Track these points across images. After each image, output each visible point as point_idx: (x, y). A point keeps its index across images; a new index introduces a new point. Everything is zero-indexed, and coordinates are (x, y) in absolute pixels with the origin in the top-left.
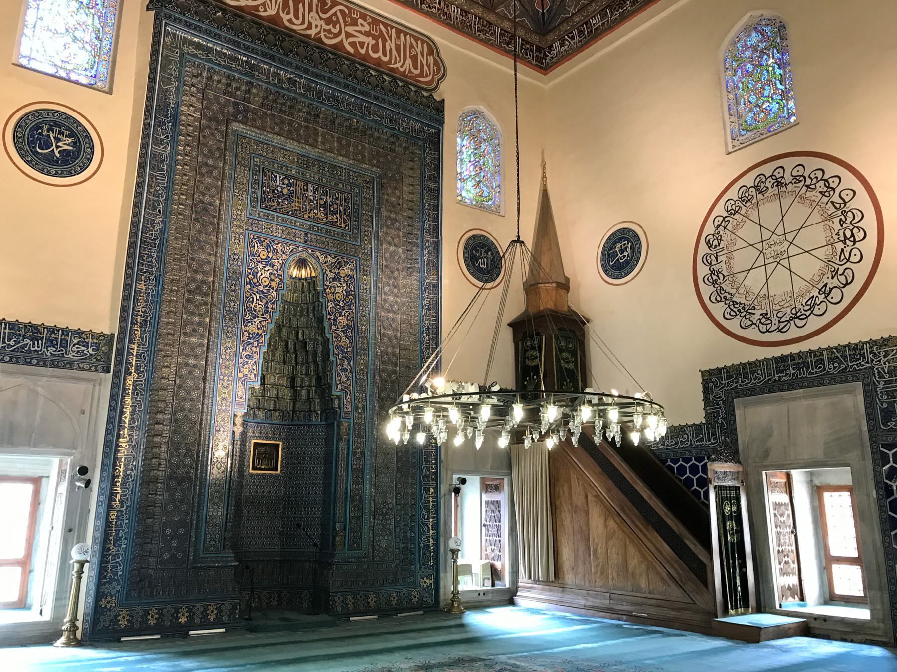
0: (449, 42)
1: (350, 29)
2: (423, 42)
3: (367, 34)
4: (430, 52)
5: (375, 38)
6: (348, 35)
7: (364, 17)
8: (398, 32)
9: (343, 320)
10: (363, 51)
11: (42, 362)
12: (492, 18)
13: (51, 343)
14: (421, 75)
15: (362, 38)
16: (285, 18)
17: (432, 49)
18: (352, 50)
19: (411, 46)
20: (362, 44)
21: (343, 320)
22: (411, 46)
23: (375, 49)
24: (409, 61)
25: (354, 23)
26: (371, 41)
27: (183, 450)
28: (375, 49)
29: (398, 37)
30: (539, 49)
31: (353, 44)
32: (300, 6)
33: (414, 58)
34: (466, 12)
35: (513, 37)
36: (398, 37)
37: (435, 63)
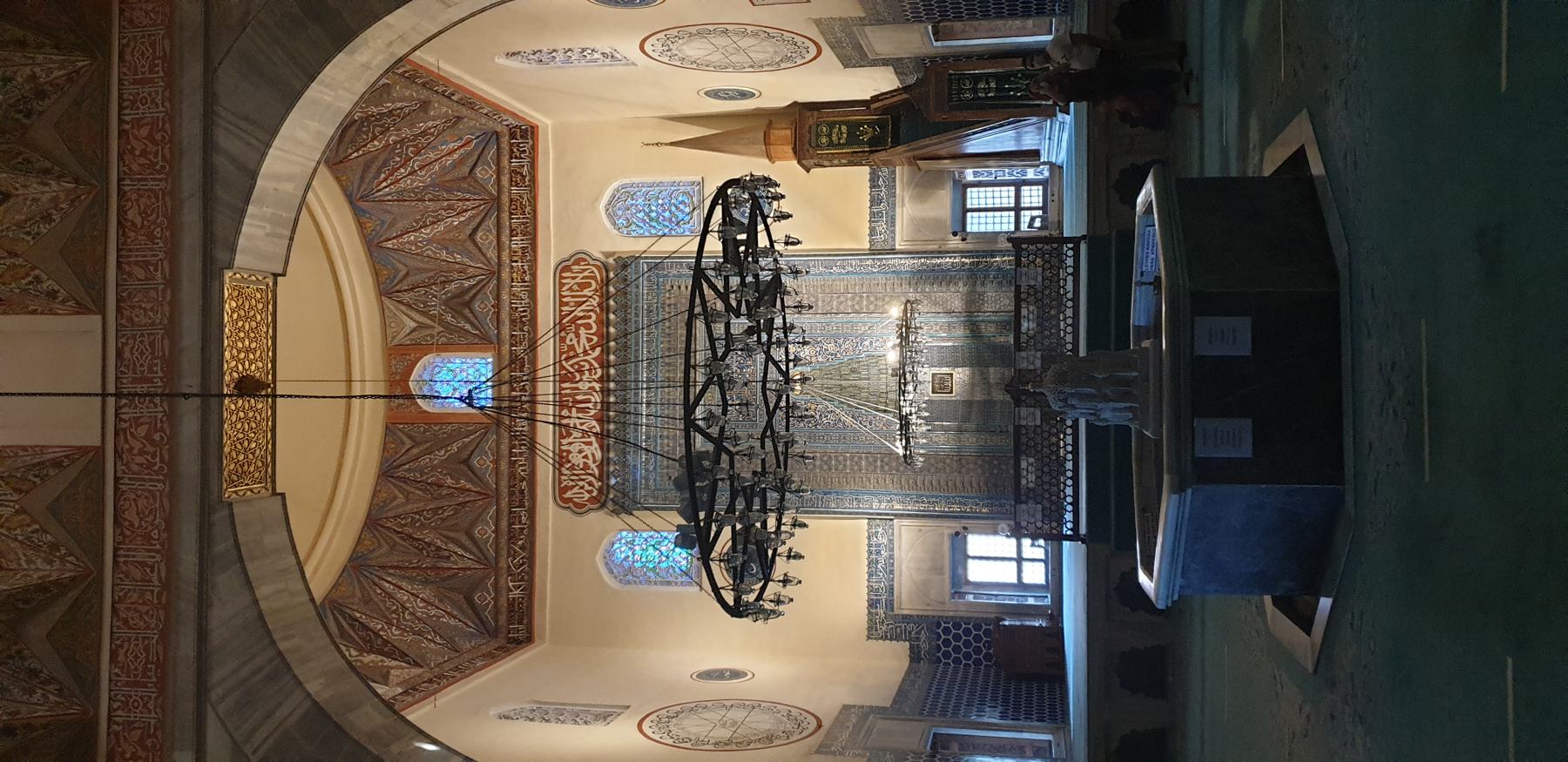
0: (550, 255)
1: (580, 350)
2: (562, 278)
3: (578, 336)
4: (567, 269)
5: (578, 327)
6: (585, 352)
7: (563, 340)
8: (562, 304)
9: (831, 347)
10: (595, 339)
11: (891, 557)
12: (505, 199)
13: (878, 553)
14: (594, 278)
15: (583, 340)
16: (593, 412)
17: (563, 268)
18: (598, 350)
19: (570, 289)
20: (589, 340)
21: (831, 347)
22: (570, 289)
23: (588, 326)
24: (586, 292)
25: (571, 348)
26: (582, 331)
27: (940, 465)
28: (588, 326)
29: (567, 304)
30: (512, 136)
31: (593, 349)
32: (579, 398)
33: (582, 286)
34: (512, 231)
35: (514, 172)
36: (567, 304)
37: (577, 262)
